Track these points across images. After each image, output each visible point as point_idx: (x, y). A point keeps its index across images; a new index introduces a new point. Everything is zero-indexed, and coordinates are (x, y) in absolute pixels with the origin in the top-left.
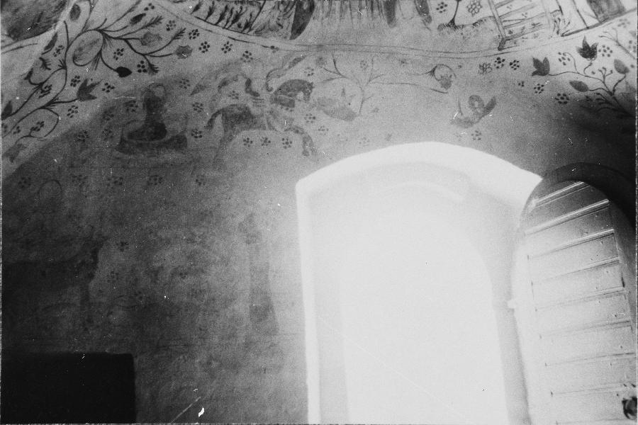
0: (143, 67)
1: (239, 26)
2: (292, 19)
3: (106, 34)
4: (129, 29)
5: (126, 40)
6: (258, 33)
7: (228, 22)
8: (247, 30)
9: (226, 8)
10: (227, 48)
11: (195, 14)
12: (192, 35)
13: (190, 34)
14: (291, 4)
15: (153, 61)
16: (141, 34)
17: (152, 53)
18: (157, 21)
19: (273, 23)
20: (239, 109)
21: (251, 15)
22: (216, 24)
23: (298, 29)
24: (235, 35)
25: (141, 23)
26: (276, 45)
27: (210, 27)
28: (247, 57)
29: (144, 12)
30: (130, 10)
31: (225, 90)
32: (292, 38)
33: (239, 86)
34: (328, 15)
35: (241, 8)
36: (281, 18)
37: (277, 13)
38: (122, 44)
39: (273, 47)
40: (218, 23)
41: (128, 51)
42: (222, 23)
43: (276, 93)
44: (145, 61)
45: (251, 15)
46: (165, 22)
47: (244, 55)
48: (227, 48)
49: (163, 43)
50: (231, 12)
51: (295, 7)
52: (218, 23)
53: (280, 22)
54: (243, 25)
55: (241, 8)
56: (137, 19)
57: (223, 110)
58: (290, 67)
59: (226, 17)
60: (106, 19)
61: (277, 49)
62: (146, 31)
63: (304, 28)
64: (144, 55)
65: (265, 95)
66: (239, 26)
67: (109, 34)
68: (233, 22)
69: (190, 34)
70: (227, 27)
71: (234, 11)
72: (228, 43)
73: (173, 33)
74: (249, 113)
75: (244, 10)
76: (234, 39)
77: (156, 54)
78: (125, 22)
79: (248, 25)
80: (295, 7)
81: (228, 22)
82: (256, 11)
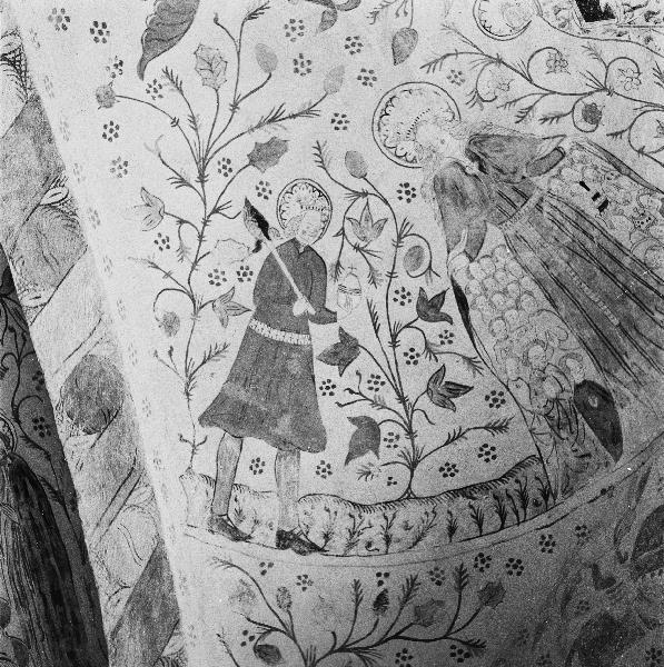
0: (460, 652)
1: (536, 504)
3: (355, 649)
4: (384, 622)
5: (397, 636)
6: (568, 491)
7: (516, 513)
8: (551, 499)
9: (496, 498)
10: (547, 544)
11: (458, 535)
12: (480, 566)
13: (476, 566)
15: (468, 634)
16: (407, 615)
17: (451, 628)
18: (412, 583)
19: (572, 459)
20: (596, 625)
21: (537, 478)
22: (502, 528)
23: (612, 438)
24: (543, 519)
25: (394, 603)
26: (605, 484)
27: (494, 538)
28: (583, 534)
29: (381, 589)
30: (358, 601)
31: (571, 609)
32: (617, 460)
33: (587, 590)
34: (638, 383)
36: (576, 446)
38: (397, 645)
39: (603, 492)
40: (503, 523)
41: (412, 647)
42: (511, 517)
43: (634, 558)
44: (455, 643)
45: (537, 478)
46: (423, 578)
47: (578, 535)
48: (547, 544)
49: (451, 604)
50: (509, 497)
52: (503, 523)
53: (581, 451)
55: (517, 481)
56: (381, 602)
57: (576, 643)
58: (638, 500)
59: (508, 509)
60: (333, 633)
61: (612, 487)
62: (409, 608)
63: (619, 428)
64: (445, 637)
65: (622, 574)
66: (536, 504)
67: (362, 644)
68: (524, 507)
69: (476, 566)
71: (511, 492)
72: (543, 537)
73: (451, 581)
74: (612, 620)
75: (522, 480)
76: (547, 526)
77: (460, 622)
78: (367, 617)
79: (546, 493)
80: (580, 416)
81: (516, 513)
82: (538, 469)
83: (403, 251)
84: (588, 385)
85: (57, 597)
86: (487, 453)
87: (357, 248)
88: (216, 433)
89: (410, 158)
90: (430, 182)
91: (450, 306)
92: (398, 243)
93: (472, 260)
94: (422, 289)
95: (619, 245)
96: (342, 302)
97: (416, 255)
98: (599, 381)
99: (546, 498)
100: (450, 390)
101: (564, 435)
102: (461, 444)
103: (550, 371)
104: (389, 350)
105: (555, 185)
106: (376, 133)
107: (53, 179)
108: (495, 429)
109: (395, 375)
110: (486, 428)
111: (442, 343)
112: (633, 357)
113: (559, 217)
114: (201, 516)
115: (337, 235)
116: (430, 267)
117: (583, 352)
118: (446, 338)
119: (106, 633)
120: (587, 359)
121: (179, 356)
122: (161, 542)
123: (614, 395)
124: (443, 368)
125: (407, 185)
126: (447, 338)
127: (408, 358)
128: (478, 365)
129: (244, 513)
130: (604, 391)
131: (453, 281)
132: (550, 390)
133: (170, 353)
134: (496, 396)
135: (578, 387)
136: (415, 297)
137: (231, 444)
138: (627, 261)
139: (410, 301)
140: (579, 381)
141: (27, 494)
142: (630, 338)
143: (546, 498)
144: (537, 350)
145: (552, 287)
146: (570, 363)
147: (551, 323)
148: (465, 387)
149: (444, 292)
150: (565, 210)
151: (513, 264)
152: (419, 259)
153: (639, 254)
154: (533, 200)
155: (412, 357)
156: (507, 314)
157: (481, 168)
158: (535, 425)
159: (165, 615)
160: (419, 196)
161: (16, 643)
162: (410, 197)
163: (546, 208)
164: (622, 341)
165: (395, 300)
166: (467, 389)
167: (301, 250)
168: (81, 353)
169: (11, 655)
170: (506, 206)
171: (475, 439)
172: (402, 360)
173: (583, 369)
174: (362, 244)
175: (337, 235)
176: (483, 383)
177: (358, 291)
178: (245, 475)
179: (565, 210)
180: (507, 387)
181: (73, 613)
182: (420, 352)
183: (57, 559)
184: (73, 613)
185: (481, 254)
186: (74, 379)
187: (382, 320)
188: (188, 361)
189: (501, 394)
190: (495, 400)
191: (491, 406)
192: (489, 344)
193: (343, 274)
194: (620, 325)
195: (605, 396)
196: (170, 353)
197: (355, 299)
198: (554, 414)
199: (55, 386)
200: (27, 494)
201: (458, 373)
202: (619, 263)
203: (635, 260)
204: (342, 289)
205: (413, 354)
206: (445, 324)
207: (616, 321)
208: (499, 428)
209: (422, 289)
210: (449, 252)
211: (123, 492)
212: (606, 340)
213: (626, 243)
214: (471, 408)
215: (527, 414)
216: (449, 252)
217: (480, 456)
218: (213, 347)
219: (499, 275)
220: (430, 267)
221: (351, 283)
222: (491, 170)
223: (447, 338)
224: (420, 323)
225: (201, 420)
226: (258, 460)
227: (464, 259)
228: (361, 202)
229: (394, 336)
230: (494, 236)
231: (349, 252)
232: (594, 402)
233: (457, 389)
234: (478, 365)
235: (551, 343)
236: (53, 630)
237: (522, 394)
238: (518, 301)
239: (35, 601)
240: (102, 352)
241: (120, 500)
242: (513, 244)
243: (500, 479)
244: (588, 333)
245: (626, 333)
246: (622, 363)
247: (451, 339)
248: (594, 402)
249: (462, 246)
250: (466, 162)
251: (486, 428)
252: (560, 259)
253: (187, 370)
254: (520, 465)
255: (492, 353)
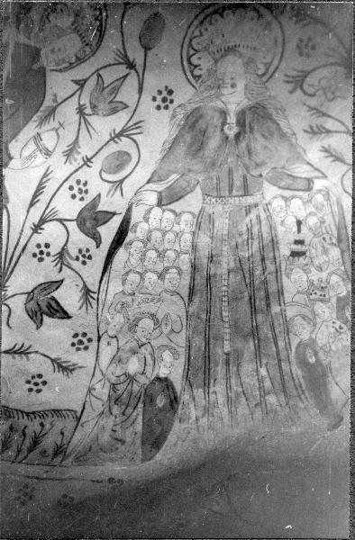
2: (139, 427)
8: (59, 459)
9: (11, 429)
10: (26, 494)
14: (133, 402)
19: (105, 438)
21: (62, 433)
32: (143, 461)
35: (42, 425)
36: (118, 428)
37: (109, 422)
51: (140, 405)
53: (119, 435)
54: (50, 451)
55: (42, 425)
63: (165, 438)
68: (30, 450)
70: (18, 459)
71: (29, 432)
75: (48, 426)
80: (140, 405)
81: (19, 451)
82: (69, 424)
83: (113, 148)
84: (166, 383)
86: (36, 384)
87: (81, 110)
89: (197, 72)
90: (190, 108)
91: (108, 232)
92: (116, 137)
93: (159, 204)
94: (99, 195)
95: (280, 292)
96: (27, 152)
97: (121, 160)
98: (178, 387)
99: (56, 454)
100: (49, 306)
101: (116, 410)
102: (19, 361)
103: (146, 351)
104: (28, 232)
105: (278, 203)
106: (196, 23)
108: (60, 366)
109: (13, 262)
110: (53, 360)
111: (77, 259)
112: (219, 389)
113: (255, 230)
115: (76, 82)
116: (121, 182)
117: (182, 351)
118: (84, 256)
120: (182, 360)
123: (180, 407)
124: (59, 283)
125: (170, 92)
126: (85, 257)
127: (37, 251)
128: (91, 300)
130: (175, 398)
131: (129, 210)
132: (133, 366)
134: (85, 340)
135: (158, 379)
136: (89, 198)
138: (275, 309)
139: (82, 199)
140: (162, 375)
142: (228, 370)
143: (56, 454)
144: (147, 323)
145: (200, 280)
146: (167, 356)
147: (174, 309)
148: (66, 313)
149: (114, 214)
150: (265, 229)
151: (188, 237)
152: (120, 167)
153: (290, 314)
154: (250, 200)
155: (42, 253)
156: (149, 275)
157: (238, 136)
158: (98, 386)
160: (170, 111)
162: (162, 105)
163: (253, 216)
164: (219, 368)
165: (71, 188)
166: (66, 315)
167: (35, 67)
170: (224, 185)
171: (35, 364)
172: (32, 248)
173: (171, 367)
174: (88, 111)
175: (76, 82)
176: (83, 320)
177: (48, 153)
179: (265, 229)
180: (99, 338)
182: (52, 254)
185: (169, 207)
187: (44, 198)
189: (90, 340)
190: (80, 342)
191: (73, 345)
192: (114, 287)
193: (53, 124)
194: (228, 354)
195: (174, 401)
197: (40, 158)
198: (121, 388)
201: (68, 297)
202: (268, 305)
203: (283, 313)
204: (37, 138)
205: (45, 250)
206: (91, 243)
207: (227, 348)
208: (63, 367)
209: (99, 195)
210: (148, 182)
212: (207, 359)
213: (288, 297)
214: (55, 334)
215: (98, 373)
216: (148, 182)
217: (29, 382)
219: (170, 236)
220: (121, 182)
221: (49, 140)
222: (243, 145)
223: (85, 257)
224: (73, 226)
227: (152, 198)
228: (123, 70)
229: (43, 221)
230: (193, 202)
231: (72, 106)
232: (161, 402)
233: (58, 311)
234: (91, 300)
235: (163, 327)
237: (107, 352)
238: (166, 270)
242: (202, 221)
243: (28, 414)
244: (198, 342)
245: (227, 363)
246: (206, 385)
247: (87, 260)
248: (161, 402)
249: (161, 187)
250: (232, 119)
251: (53, 360)
252: (227, 262)
254: (57, 412)
255: (110, 298)
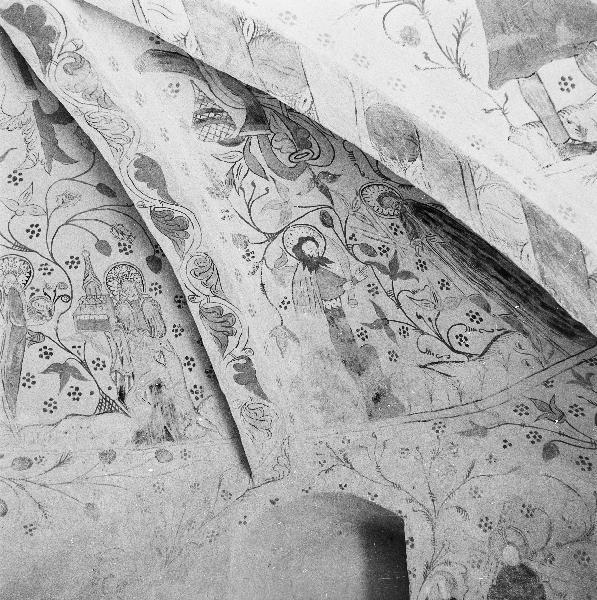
85: (502, 272)
88: (510, 86)
107: (239, 22)
114: (550, 154)
119: (538, 282)
121: (436, 55)
122: (522, 198)
129: (583, 126)
133: (427, 58)
137: (532, 83)
141: (433, 221)
159: (565, 244)
161: (506, 319)
168: (361, 113)
169: (508, 327)
178: (562, 100)
181: (522, 278)
183: (484, 249)
184: (522, 278)
186: (373, 133)
188: (445, 50)
196: (427, 58)
199: (368, 147)
200: (433, 221)
211: (468, 182)
218: (457, 25)
225: (491, 86)
226: (563, 79)
236: (520, 296)
239: (493, 284)
240: (371, 102)
241: (470, 189)
253: (450, 59)
